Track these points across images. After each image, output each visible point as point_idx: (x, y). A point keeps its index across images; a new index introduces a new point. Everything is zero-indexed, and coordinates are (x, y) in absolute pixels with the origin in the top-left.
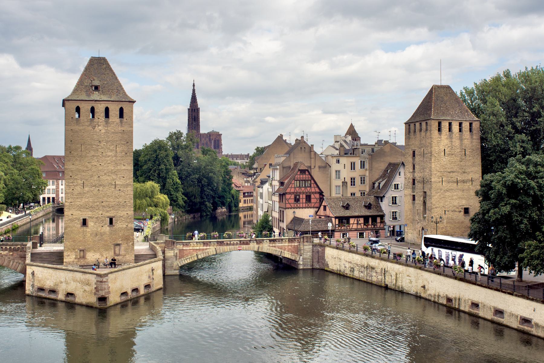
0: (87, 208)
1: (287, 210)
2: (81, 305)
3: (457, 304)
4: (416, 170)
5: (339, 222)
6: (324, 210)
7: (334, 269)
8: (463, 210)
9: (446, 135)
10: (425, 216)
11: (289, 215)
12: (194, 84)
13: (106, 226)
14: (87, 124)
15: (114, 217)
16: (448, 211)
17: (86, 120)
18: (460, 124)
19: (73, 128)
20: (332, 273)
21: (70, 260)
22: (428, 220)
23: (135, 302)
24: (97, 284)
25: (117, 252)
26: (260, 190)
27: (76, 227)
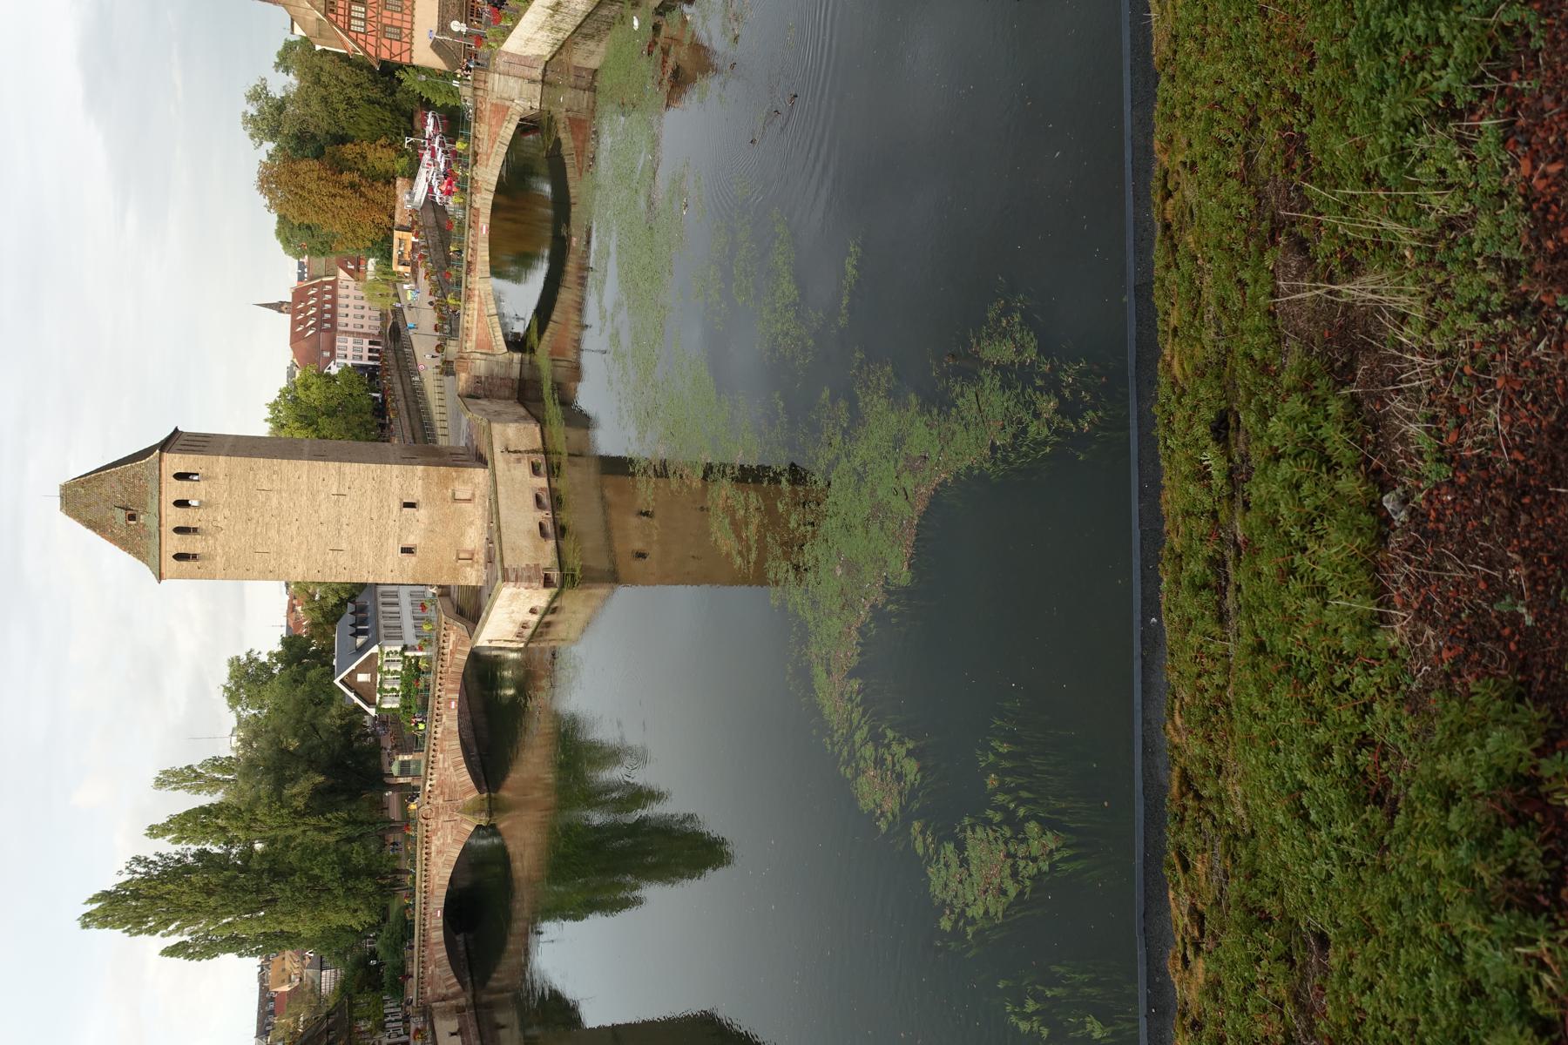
14: (211, 542)
23: (557, 501)
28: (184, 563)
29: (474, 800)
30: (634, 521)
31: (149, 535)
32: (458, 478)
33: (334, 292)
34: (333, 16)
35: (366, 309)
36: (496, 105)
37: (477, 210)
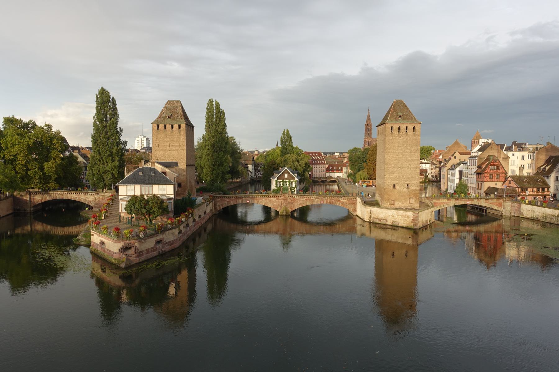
1: (485, 183)
2: (402, 227)
6: (509, 183)
11: (487, 185)
12: (369, 109)
20: (527, 219)
26: (451, 171)
29: (288, 210)
30: (404, 252)
31: (396, 120)
33: (322, 164)
34: (493, 162)
36: (502, 204)
37: (473, 201)
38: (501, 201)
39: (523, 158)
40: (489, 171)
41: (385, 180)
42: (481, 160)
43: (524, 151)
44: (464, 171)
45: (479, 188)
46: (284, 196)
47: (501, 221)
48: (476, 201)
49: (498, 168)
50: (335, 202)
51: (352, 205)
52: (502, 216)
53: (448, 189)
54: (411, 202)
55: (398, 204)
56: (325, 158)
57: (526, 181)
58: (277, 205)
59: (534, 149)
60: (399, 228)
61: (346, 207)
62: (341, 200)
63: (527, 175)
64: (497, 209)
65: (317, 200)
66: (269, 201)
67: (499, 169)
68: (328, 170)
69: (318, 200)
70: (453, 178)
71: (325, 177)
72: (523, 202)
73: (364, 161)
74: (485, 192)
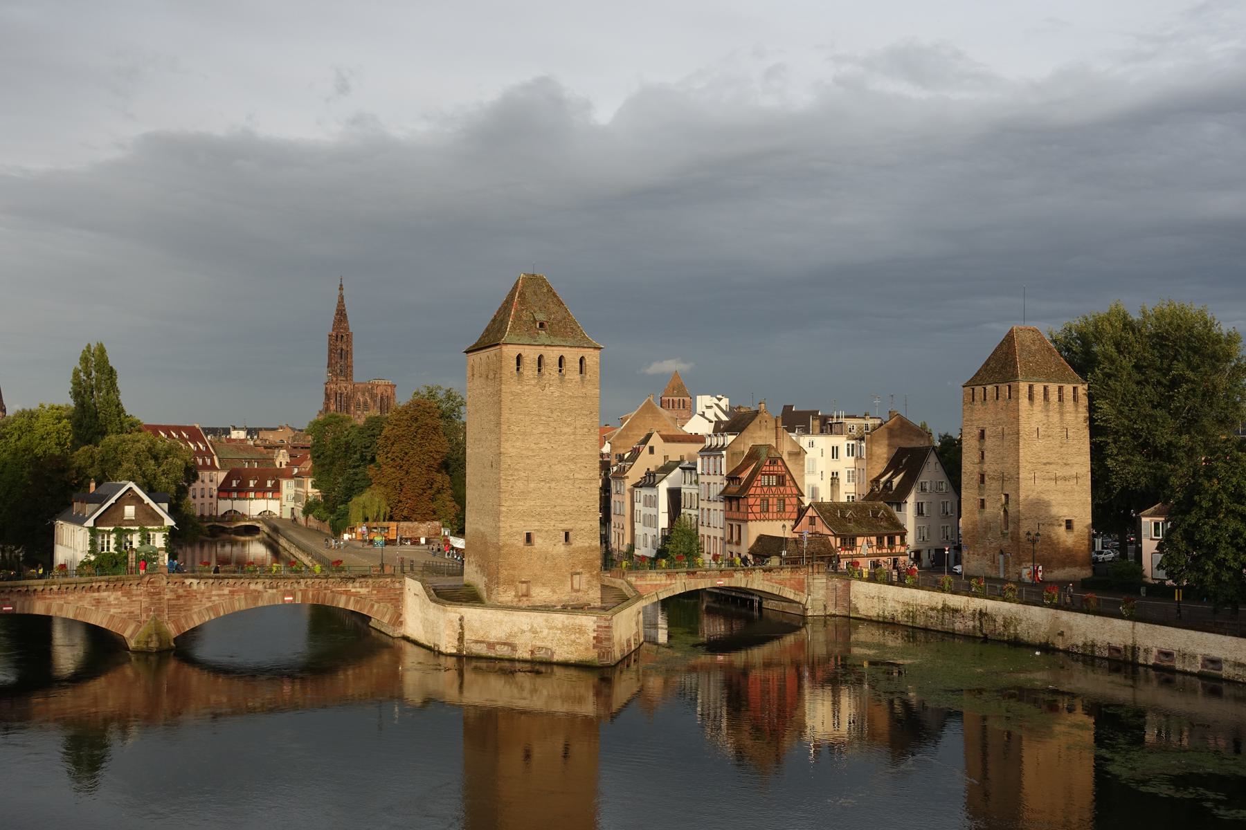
0: (533, 516)
1: (749, 523)
2: (565, 665)
3: (1129, 655)
4: (986, 459)
5: (841, 543)
7: (871, 614)
8: (1064, 524)
9: (1041, 405)
10: (1005, 531)
11: (756, 529)
12: (341, 285)
13: (561, 544)
14: (533, 382)
15: (572, 530)
16: (1043, 524)
17: (532, 376)
18: (1060, 389)
19: (513, 389)
20: (869, 621)
21: (507, 599)
22: (1012, 538)
24: (597, 631)
25: (576, 586)
26: (645, 492)
27: (516, 546)
28: (515, 362)
29: (167, 633)
32: (592, 576)
34: (768, 463)
35: (201, 500)
36: (803, 582)
37: (733, 576)
38: (801, 575)
39: (835, 452)
40: (758, 491)
41: (503, 519)
42: (735, 459)
43: (837, 434)
44: (687, 493)
45: (733, 538)
46: (153, 582)
47: (804, 631)
48: (741, 578)
49: (781, 481)
50: (333, 598)
51: (389, 605)
52: (804, 617)
53: (637, 545)
54: (576, 586)
55: (541, 594)
56: (212, 445)
57: (851, 517)
58: (125, 616)
59: (860, 429)
60: (556, 669)
61: (369, 612)
62: (353, 590)
63: (846, 500)
64: (791, 597)
65: (270, 591)
66: (94, 602)
67: (783, 484)
68: (225, 490)
69: (275, 591)
70: (652, 511)
71: (214, 514)
72: (856, 575)
73: (368, 458)
74: (751, 551)
